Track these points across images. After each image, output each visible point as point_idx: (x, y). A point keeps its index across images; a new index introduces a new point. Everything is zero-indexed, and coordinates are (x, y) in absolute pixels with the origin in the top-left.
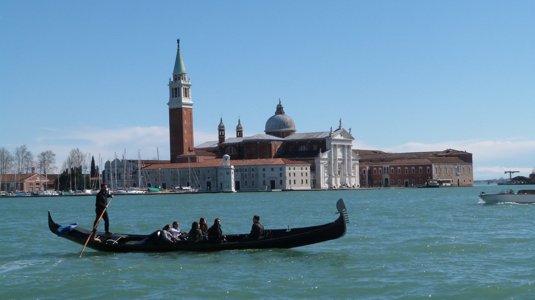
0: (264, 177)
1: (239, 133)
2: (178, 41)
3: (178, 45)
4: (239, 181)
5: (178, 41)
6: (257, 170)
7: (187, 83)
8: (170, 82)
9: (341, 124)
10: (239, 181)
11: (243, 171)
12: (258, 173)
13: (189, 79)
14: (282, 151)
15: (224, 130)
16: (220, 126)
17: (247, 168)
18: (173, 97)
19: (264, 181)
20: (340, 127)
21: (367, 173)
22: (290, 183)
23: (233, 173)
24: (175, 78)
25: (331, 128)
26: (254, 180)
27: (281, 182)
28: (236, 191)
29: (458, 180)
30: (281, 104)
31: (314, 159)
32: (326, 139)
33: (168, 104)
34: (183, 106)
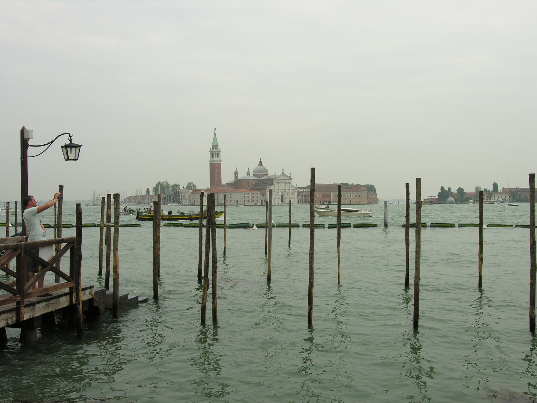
2: (215, 129)
3: (215, 132)
5: (215, 129)
7: (218, 150)
9: (283, 171)
14: (257, 185)
15: (237, 174)
16: (235, 172)
20: (282, 172)
21: (304, 196)
22: (245, 201)
25: (276, 173)
29: (351, 201)
30: (261, 160)
31: (265, 189)
32: (273, 179)
34: (215, 162)
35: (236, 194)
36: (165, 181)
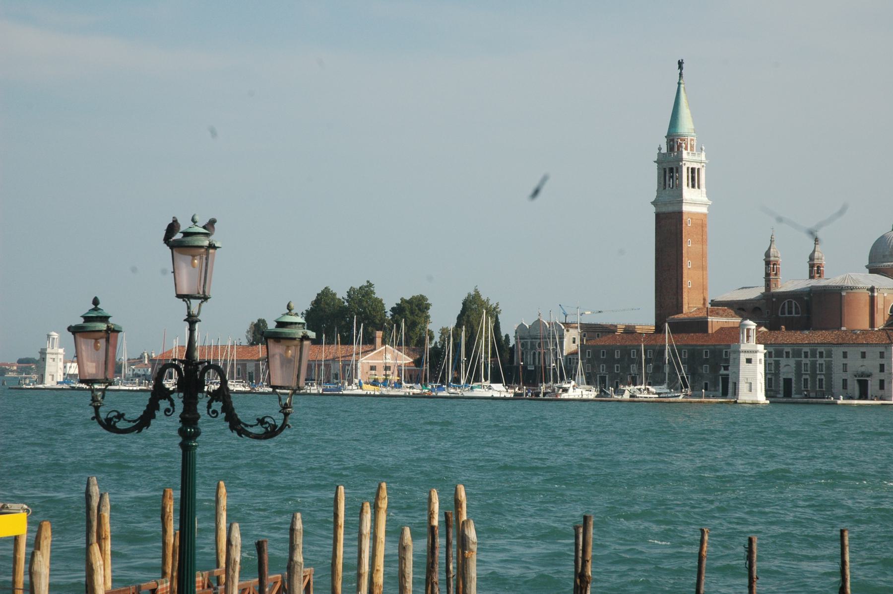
0: (845, 370)
1: (815, 269)
3: (681, 74)
4: (791, 379)
6: (829, 355)
7: (696, 158)
8: (659, 154)
10: (791, 379)
11: (801, 357)
12: (832, 361)
13: (702, 149)
17: (809, 351)
18: (665, 189)
19: (845, 381)
23: (763, 361)
24: (670, 146)
26: (823, 377)
27: (882, 384)
28: (768, 402)
33: (654, 203)
34: (686, 208)
35: (854, 353)
36: (366, 284)
